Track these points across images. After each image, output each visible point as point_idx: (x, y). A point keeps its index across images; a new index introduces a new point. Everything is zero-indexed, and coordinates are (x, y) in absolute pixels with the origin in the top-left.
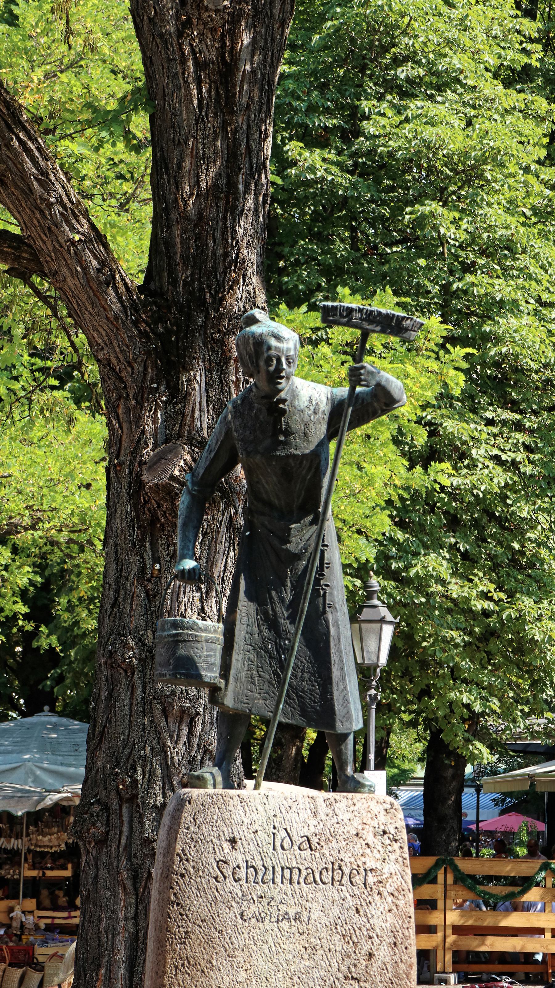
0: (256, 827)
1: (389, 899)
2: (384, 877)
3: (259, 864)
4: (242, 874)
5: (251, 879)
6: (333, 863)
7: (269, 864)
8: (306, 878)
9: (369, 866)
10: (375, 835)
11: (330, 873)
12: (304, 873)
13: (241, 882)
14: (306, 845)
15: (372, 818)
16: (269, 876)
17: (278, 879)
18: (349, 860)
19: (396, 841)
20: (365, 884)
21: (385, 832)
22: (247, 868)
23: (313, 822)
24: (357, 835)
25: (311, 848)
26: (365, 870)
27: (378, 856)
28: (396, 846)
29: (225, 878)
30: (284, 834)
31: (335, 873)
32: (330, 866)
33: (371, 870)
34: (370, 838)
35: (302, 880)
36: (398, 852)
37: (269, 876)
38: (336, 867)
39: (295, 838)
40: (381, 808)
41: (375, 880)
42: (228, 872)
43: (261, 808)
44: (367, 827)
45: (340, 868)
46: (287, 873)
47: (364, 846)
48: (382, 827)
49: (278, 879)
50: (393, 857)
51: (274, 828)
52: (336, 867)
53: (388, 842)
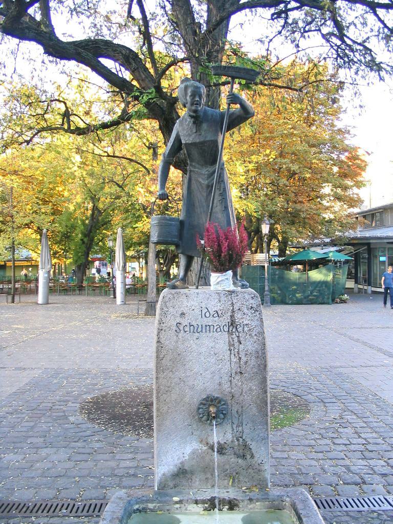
0: (193, 308)
1: (255, 337)
2: (252, 327)
3: (194, 323)
4: (187, 329)
5: (192, 331)
7: (199, 324)
8: (216, 330)
9: (245, 323)
12: (216, 328)
13: (187, 333)
14: (216, 315)
16: (199, 330)
17: (204, 331)
19: (257, 311)
20: (243, 331)
21: (252, 307)
22: (190, 326)
23: (219, 304)
24: (239, 309)
25: (218, 316)
27: (248, 318)
28: (257, 313)
29: (180, 330)
32: (227, 324)
34: (246, 311)
35: (214, 330)
36: (258, 316)
37: (199, 330)
39: (211, 312)
40: (250, 296)
42: (181, 328)
43: (195, 299)
46: (208, 327)
47: (243, 314)
49: (204, 331)
50: (256, 318)
51: (202, 308)
53: (253, 312)
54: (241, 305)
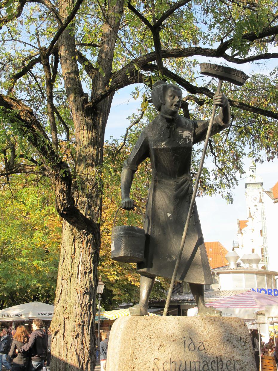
6: (217, 357)
8: (203, 368)
10: (237, 341)
11: (216, 363)
15: (234, 330)
18: (226, 355)
26: (234, 361)
30: (190, 341)
31: (219, 364)
33: (238, 360)
34: (235, 343)
38: (219, 360)
41: (240, 366)
44: (233, 335)
45: (221, 361)
48: (240, 335)
50: (247, 352)
52: (219, 360)
54: (229, 335)
